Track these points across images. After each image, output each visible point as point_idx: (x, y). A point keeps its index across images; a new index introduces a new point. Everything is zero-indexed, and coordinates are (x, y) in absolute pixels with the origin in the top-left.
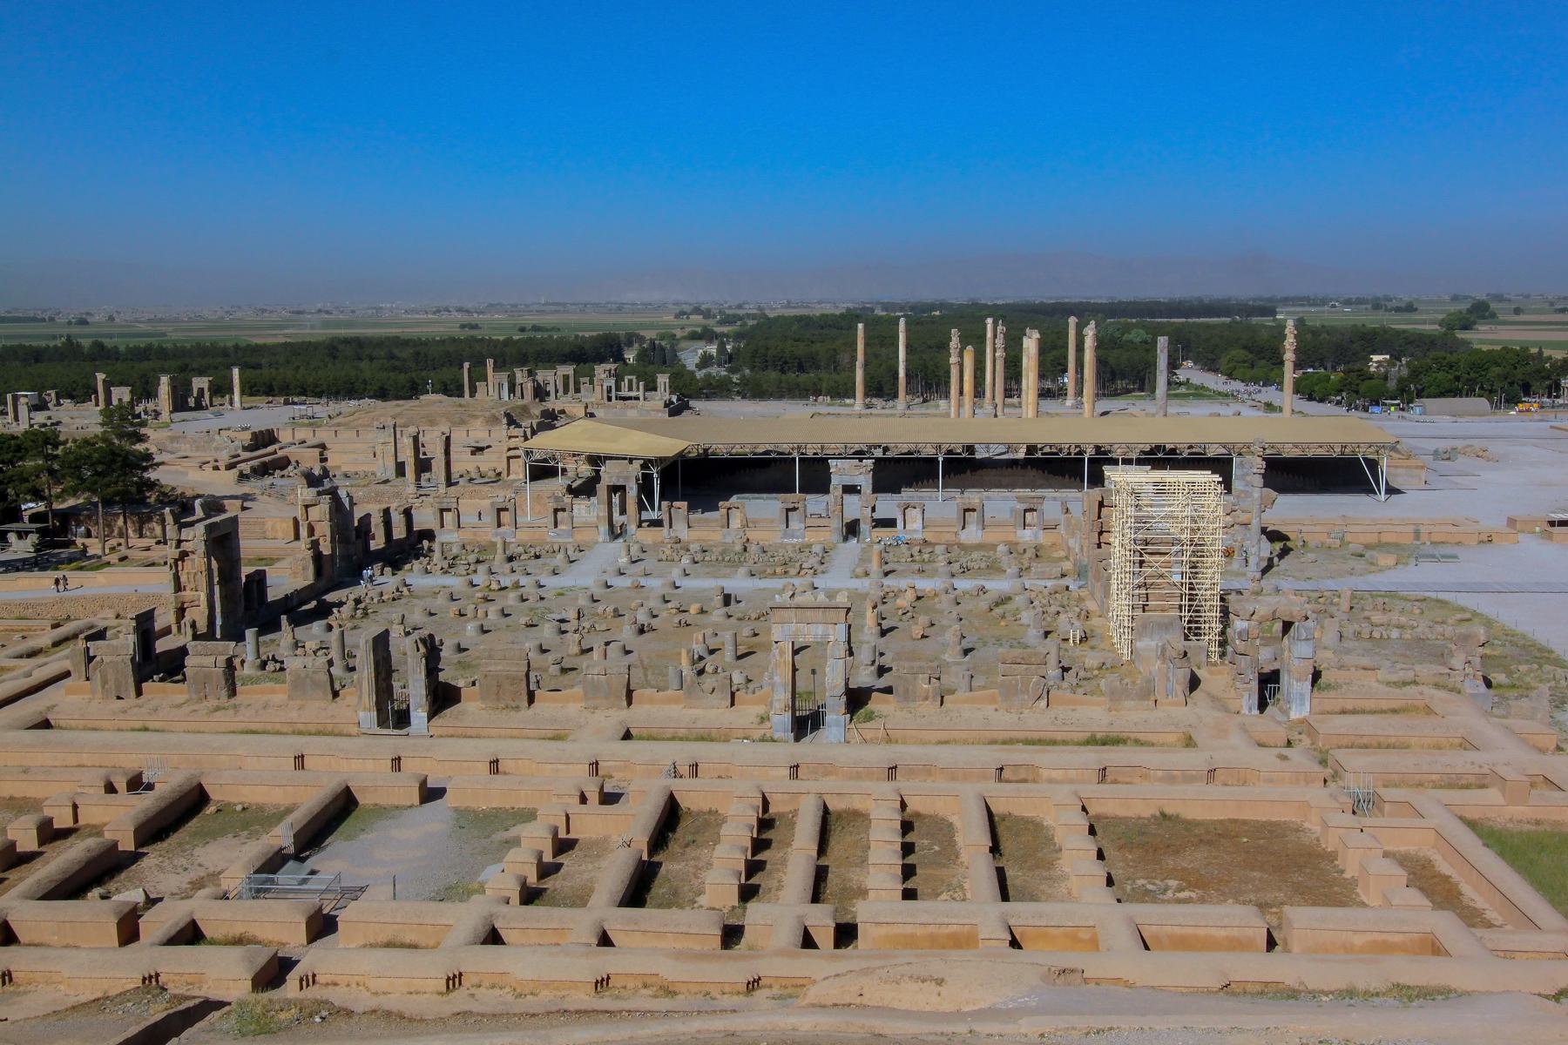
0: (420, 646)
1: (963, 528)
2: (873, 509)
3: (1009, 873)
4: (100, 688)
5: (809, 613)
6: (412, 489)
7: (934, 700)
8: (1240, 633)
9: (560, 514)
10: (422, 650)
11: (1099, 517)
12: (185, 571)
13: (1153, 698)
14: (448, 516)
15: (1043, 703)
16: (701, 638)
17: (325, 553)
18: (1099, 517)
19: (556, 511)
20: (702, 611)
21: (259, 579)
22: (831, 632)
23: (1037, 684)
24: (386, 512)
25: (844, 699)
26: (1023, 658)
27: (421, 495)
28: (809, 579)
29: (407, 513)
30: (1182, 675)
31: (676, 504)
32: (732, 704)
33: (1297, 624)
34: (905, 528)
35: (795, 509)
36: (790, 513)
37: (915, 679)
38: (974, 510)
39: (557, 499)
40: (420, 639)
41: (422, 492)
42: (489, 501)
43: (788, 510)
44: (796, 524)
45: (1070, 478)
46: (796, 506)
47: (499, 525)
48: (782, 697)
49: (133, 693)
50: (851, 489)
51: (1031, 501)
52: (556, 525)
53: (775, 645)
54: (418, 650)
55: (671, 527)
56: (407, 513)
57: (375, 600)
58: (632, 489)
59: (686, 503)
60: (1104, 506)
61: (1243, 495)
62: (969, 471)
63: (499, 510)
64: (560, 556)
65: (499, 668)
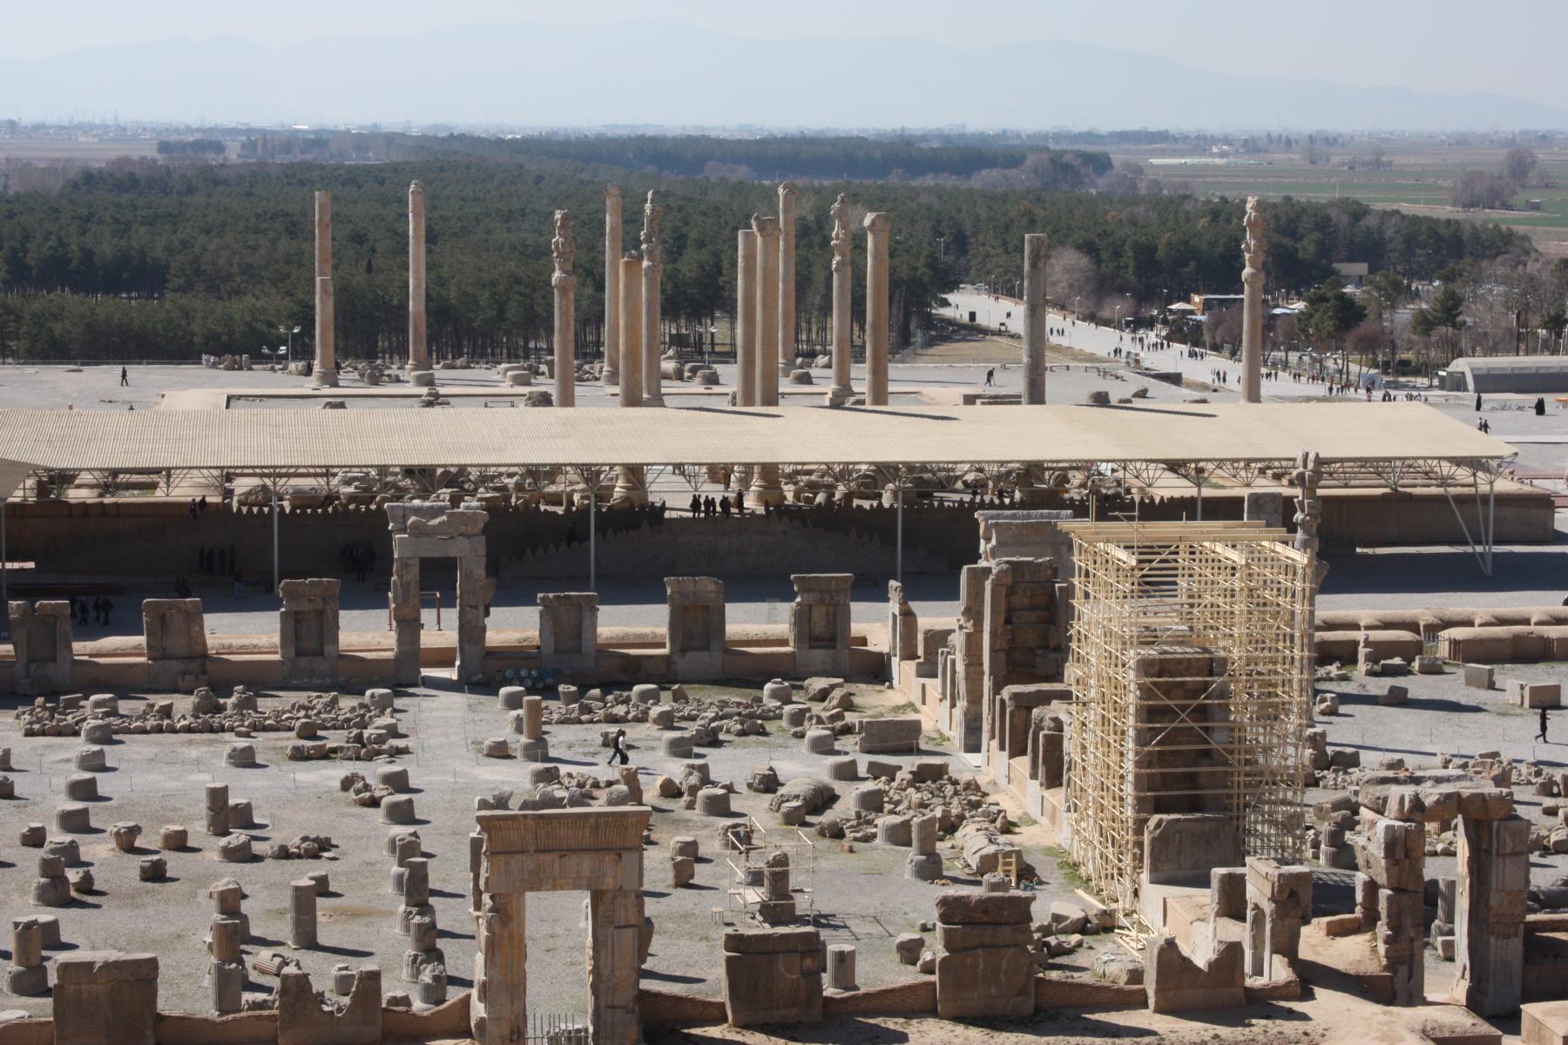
2: (487, 614)
28: (382, 767)
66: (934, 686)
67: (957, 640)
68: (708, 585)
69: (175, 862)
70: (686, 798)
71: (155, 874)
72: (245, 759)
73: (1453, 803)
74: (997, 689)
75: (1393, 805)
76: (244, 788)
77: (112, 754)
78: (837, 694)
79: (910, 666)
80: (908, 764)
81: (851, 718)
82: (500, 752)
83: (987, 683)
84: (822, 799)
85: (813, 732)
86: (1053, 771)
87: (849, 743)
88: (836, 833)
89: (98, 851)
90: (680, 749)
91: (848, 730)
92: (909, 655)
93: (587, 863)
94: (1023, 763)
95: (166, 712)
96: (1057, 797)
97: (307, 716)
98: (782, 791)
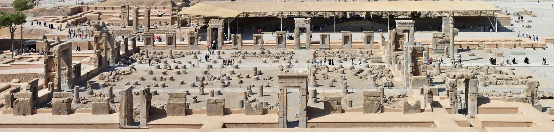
0: (145, 93)
2: (311, 37)
6: (134, 31)
10: (146, 94)
16: (249, 88)
17: (103, 56)
20: (248, 77)
21: (78, 67)
24: (126, 40)
27: (138, 32)
29: (134, 40)
31: (237, 35)
40: (145, 90)
41: (139, 31)
42: (166, 34)
50: (303, 30)
54: (144, 94)
56: (134, 40)
57: (122, 74)
58: (220, 29)
59: (241, 35)
64: (193, 56)
65: (175, 101)
66: (386, 50)
67: (389, 43)
68: (348, 33)
69: (245, 80)
70: (337, 71)
71: (241, 82)
72: (265, 62)
73: (462, 77)
74: (393, 52)
75: (451, 76)
76: (261, 66)
77: (243, 60)
78: (370, 52)
79: (383, 47)
80: (378, 65)
81: (371, 56)
82: (309, 62)
83: (392, 51)
84: (362, 71)
85: (364, 59)
86: (400, 67)
87: (369, 61)
88: (361, 78)
89: (234, 78)
90: (341, 61)
91: (370, 59)
92: (383, 45)
93: (297, 84)
94: (396, 65)
95: (255, 54)
96: (400, 72)
97: (278, 55)
98: (354, 70)
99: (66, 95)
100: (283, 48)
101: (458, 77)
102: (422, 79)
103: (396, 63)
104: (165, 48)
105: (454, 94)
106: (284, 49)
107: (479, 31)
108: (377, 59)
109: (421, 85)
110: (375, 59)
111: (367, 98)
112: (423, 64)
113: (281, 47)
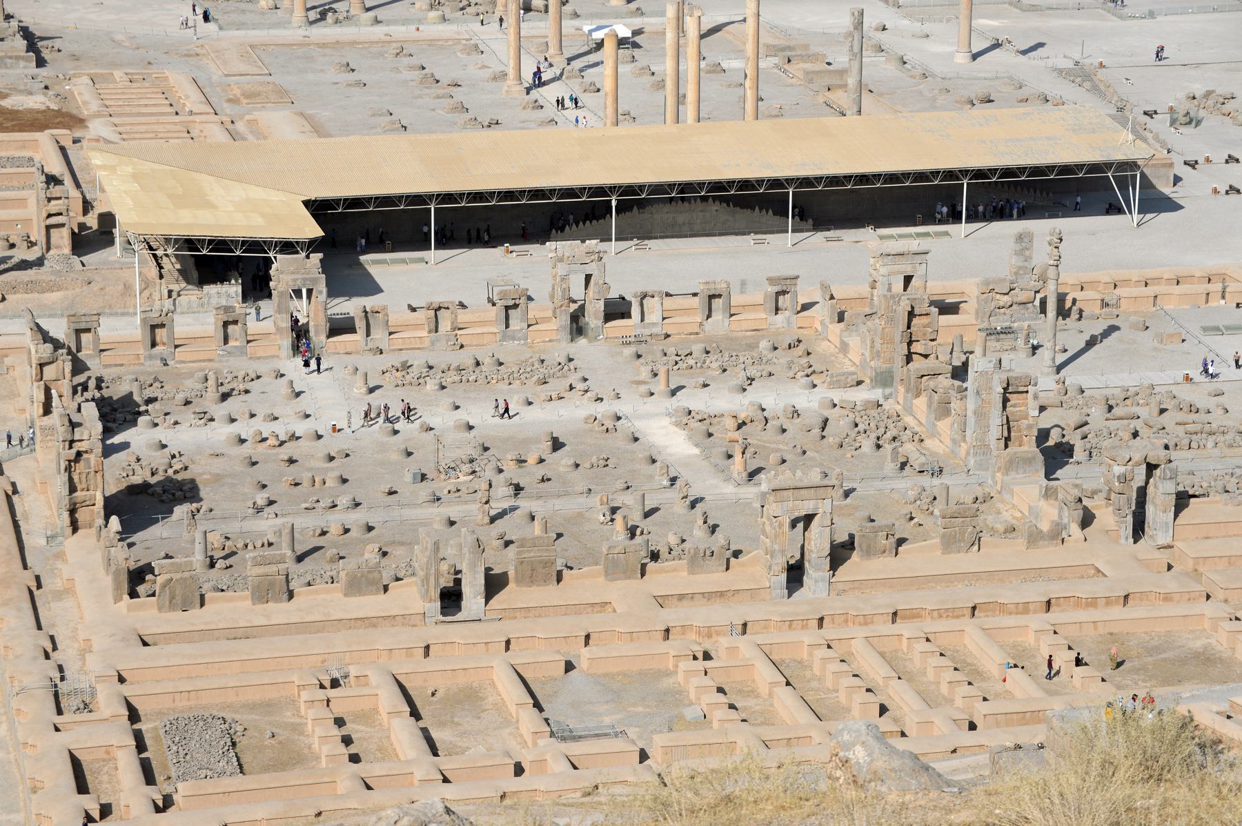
1: (709, 316)
3: (435, 735)
4: (168, 602)
5: (803, 492)
7: (891, 553)
8: (1119, 477)
9: (231, 328)
11: (909, 327)
12: (78, 471)
13: (1060, 538)
14: (85, 337)
15: (976, 547)
18: (909, 327)
19: (226, 324)
22: (820, 505)
23: (971, 533)
25: (829, 558)
26: (959, 513)
30: (1079, 514)
32: (727, 569)
33: (1163, 466)
34: (642, 320)
35: (516, 306)
36: (510, 312)
37: (876, 536)
38: (720, 296)
39: (227, 309)
43: (507, 308)
44: (516, 323)
45: (761, 210)
46: (517, 302)
47: (154, 344)
48: (780, 561)
49: (198, 605)
51: (783, 282)
52: (226, 341)
53: (774, 520)
55: (368, 334)
60: (915, 316)
61: (1021, 272)
62: (635, 208)
63: (153, 328)
65: (532, 554)
99: (278, 558)
100: (519, 339)
101: (1136, 462)
102: (1030, 455)
103: (918, 395)
104: (139, 359)
105: (1126, 499)
106: (522, 342)
107: (1044, 218)
108: (843, 378)
109: (1025, 471)
110: (839, 378)
111: (963, 522)
112: (1026, 418)
113: (513, 339)
